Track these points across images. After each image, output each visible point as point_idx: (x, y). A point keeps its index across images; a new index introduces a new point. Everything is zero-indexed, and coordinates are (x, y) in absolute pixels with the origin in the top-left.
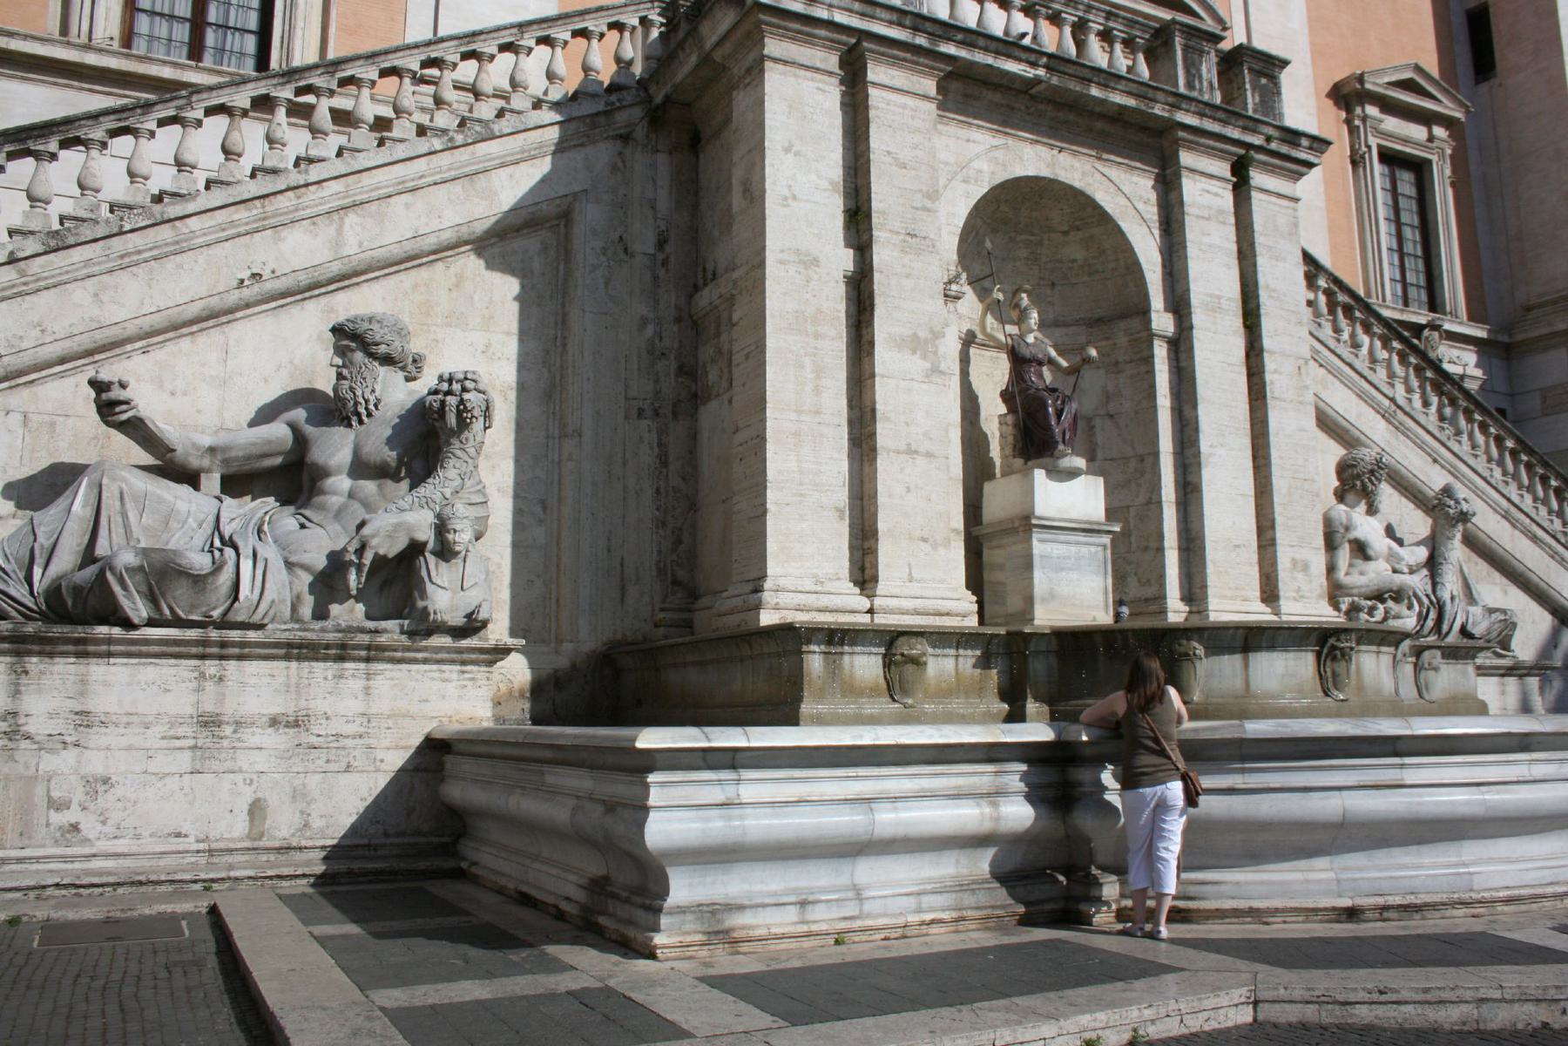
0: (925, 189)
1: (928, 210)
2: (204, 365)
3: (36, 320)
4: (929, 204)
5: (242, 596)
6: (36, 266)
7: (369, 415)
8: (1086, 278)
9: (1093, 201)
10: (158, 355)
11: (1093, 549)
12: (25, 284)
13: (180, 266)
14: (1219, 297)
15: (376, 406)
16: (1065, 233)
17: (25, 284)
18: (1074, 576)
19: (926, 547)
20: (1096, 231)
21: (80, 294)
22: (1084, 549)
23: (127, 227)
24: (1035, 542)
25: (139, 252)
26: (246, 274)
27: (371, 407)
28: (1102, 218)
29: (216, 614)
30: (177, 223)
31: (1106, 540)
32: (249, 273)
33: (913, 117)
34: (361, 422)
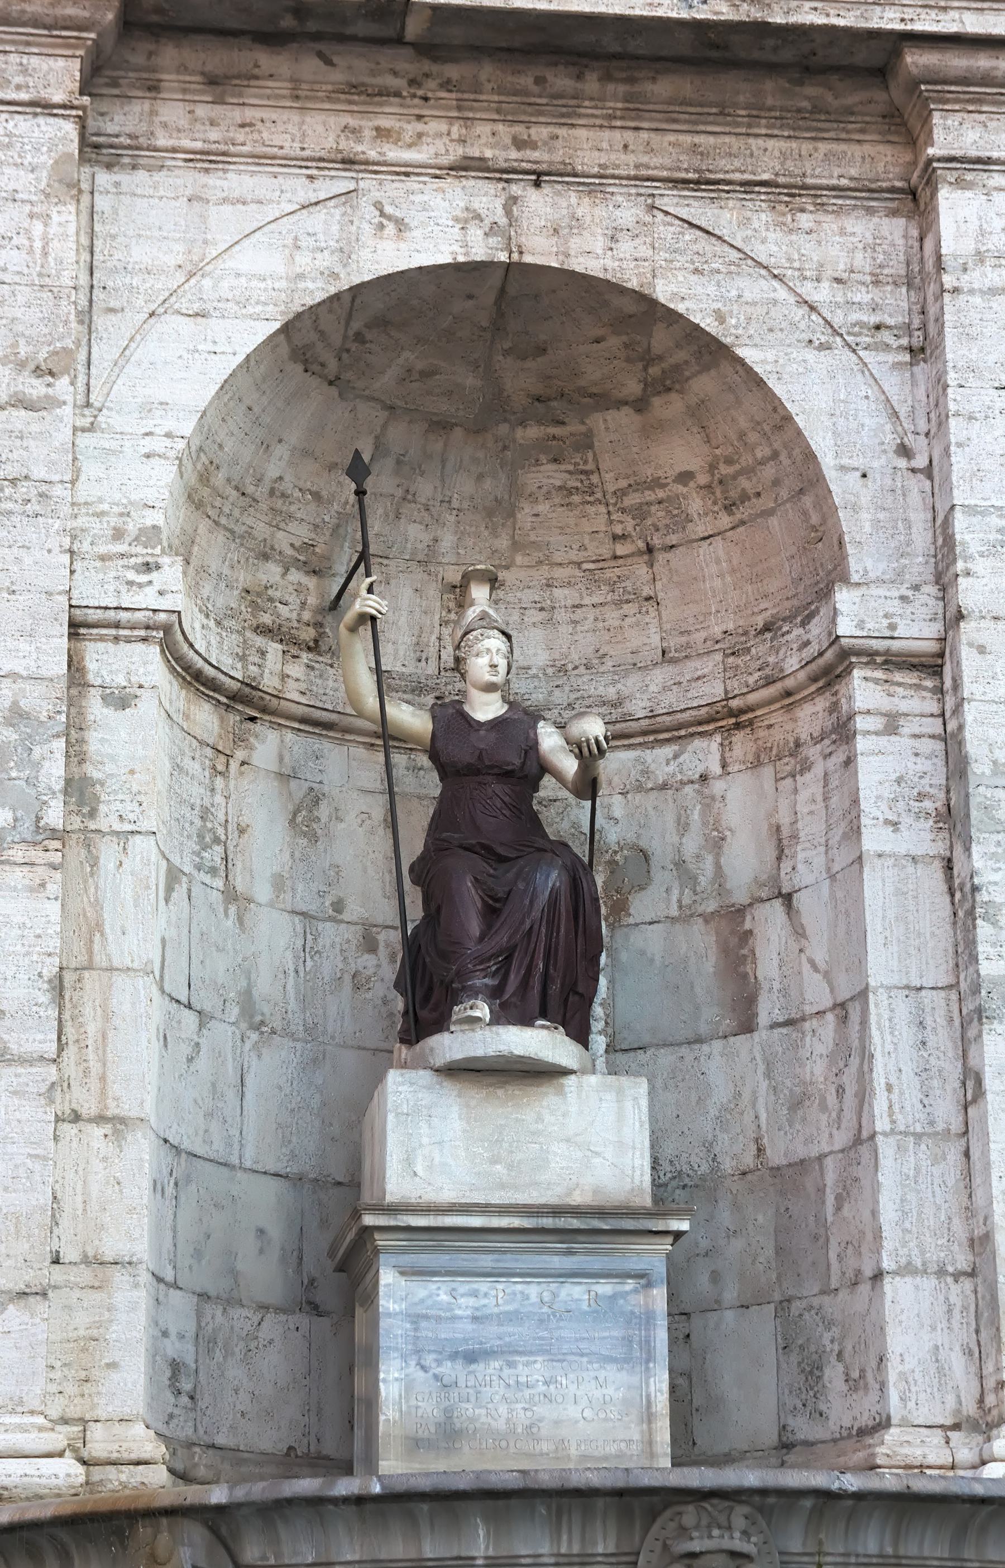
4: (36, 388)
8: (725, 520)
11: (605, 1288)
18: (534, 1371)
22: (575, 1292)
24: (387, 1277)
31: (653, 1256)
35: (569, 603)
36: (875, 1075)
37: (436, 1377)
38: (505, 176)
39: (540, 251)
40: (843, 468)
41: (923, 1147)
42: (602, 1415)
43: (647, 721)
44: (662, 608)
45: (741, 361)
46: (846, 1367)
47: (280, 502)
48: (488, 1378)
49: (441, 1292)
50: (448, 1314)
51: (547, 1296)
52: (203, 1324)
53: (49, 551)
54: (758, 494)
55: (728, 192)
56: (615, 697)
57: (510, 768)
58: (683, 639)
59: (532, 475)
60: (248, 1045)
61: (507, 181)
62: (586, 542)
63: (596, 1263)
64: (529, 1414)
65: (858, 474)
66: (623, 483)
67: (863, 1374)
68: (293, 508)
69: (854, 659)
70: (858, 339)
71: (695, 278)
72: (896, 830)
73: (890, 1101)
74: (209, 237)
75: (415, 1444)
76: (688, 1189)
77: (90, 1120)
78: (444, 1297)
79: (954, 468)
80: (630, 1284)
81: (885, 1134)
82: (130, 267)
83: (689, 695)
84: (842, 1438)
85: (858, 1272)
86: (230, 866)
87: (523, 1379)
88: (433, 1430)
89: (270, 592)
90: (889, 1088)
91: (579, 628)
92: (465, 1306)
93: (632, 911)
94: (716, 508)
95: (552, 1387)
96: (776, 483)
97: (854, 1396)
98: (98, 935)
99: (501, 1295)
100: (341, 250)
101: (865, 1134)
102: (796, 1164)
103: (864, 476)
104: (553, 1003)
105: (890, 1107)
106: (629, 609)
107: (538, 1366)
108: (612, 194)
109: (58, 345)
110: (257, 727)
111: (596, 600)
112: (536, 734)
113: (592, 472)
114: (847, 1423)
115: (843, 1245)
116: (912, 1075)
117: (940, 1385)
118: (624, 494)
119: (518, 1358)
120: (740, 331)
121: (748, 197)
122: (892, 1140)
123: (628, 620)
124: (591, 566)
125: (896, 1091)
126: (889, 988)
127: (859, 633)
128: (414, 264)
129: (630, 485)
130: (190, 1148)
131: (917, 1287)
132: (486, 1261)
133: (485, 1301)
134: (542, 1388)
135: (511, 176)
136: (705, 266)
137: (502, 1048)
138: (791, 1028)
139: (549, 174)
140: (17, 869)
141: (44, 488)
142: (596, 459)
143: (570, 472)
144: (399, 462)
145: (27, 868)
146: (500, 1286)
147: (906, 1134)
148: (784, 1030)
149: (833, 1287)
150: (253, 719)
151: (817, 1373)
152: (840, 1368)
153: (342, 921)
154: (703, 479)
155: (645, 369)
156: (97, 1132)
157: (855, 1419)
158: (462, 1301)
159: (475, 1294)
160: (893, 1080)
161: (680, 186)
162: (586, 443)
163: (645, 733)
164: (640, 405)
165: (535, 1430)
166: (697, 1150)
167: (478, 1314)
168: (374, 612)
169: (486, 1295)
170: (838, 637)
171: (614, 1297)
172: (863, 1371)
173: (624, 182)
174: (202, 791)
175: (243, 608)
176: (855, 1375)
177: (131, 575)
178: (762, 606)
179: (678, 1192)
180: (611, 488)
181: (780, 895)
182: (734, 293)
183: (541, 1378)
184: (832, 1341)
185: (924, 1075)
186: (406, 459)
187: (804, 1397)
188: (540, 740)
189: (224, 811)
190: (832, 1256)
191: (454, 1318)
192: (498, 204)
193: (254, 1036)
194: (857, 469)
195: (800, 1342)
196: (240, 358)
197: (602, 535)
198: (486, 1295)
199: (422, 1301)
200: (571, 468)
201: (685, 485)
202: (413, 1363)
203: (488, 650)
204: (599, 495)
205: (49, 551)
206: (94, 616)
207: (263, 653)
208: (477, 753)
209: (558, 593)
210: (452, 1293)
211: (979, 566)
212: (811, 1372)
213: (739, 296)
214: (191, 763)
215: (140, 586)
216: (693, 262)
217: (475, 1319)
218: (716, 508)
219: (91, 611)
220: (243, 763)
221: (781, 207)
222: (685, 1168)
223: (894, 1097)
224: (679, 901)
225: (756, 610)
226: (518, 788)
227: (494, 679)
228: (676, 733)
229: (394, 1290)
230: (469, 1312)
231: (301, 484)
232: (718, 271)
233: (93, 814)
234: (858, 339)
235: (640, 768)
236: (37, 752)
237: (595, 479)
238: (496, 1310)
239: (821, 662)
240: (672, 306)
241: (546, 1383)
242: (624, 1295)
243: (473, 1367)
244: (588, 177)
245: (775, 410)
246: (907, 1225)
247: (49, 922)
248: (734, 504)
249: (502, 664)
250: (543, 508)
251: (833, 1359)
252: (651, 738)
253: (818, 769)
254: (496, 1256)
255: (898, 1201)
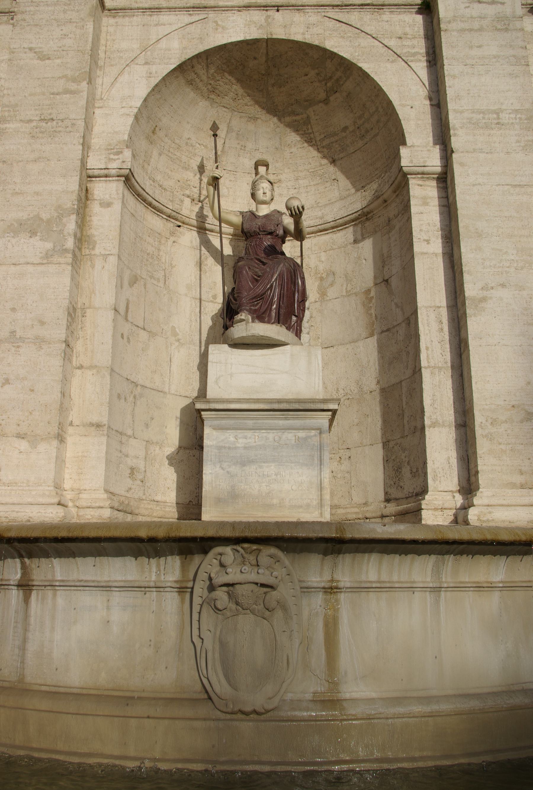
0: (69, 73)
1: (72, 92)
4: (73, 86)
8: (360, 143)
9: (325, 50)
11: (302, 434)
14: (497, 113)
16: (326, 101)
18: (271, 469)
19: (24, 445)
20: (349, 85)
22: (289, 436)
24: (207, 431)
28: (347, 67)
33: (65, 12)
35: (305, 185)
36: (421, 343)
37: (228, 472)
38: (265, 8)
39: (279, 34)
40: (404, 106)
41: (442, 373)
42: (300, 488)
43: (333, 223)
44: (339, 182)
45: (360, 69)
46: (411, 467)
47: (191, 148)
48: (250, 473)
49: (231, 437)
50: (234, 446)
51: (277, 438)
52: (149, 453)
53: (74, 145)
54: (372, 129)
55: (354, 9)
56: (321, 215)
57: (270, 231)
58: (347, 193)
59: (288, 137)
60: (173, 347)
61: (267, 10)
62: (310, 161)
63: (297, 423)
64: (268, 488)
65: (409, 107)
66: (323, 136)
67: (417, 471)
68: (197, 151)
69: (409, 176)
70: (408, 58)
71: (341, 40)
72: (428, 243)
73: (427, 354)
74: (150, 37)
75: (218, 501)
76: (350, 400)
77: (87, 368)
78: (232, 439)
79: (448, 96)
80: (313, 433)
81: (425, 368)
82: (119, 50)
83: (349, 210)
84: (409, 497)
85: (415, 427)
86: (167, 279)
87: (266, 473)
88: (226, 495)
89: (188, 182)
90: (427, 349)
91: (309, 194)
92: (241, 442)
93: (328, 295)
94: (357, 139)
95: (279, 476)
96: (378, 121)
97: (414, 479)
98: (93, 295)
99: (257, 438)
100: (201, 38)
101: (417, 369)
102: (391, 386)
103: (412, 107)
104: (281, 318)
105: (428, 356)
106: (328, 184)
107: (272, 467)
108: (308, 12)
109: (83, 70)
110: (181, 229)
111: (315, 183)
112: (281, 219)
113: (311, 133)
114: (411, 491)
115: (410, 417)
116: (437, 343)
117: (451, 473)
118: (324, 140)
119: (264, 464)
120: (359, 58)
121: (362, 10)
122: (428, 370)
123: (327, 189)
124: (313, 170)
125: (430, 349)
126: (427, 307)
127: (410, 165)
128: (230, 41)
129: (325, 136)
130: (143, 384)
131: (440, 432)
132: (250, 423)
133: (249, 440)
134: (274, 477)
135: (268, 8)
136: (345, 35)
137: (254, 332)
138: (388, 332)
139: (281, 6)
140: (53, 266)
141: (74, 122)
142: (312, 128)
143: (303, 134)
144: (237, 134)
145: (57, 265)
146: (256, 434)
147: (434, 367)
148: (386, 333)
149: (406, 435)
150: (179, 226)
151: (400, 470)
152: (409, 468)
153: (216, 303)
154: (351, 129)
155: (326, 84)
156: (89, 373)
157: (414, 489)
158: (240, 441)
159: (246, 438)
160: (429, 345)
161: (335, 8)
162: (307, 121)
163: (333, 228)
164: (326, 101)
165: (271, 495)
166: (353, 384)
167: (247, 446)
168: (217, 176)
169: (250, 438)
170: (402, 167)
171: (306, 439)
172: (417, 469)
173: (313, 8)
174: (153, 249)
175: (177, 187)
176: (414, 470)
177: (112, 156)
178: (376, 173)
179: (346, 401)
180: (318, 139)
181: (384, 280)
182: (357, 44)
183: (274, 473)
184: (405, 457)
185: (442, 343)
186: (240, 133)
187: (394, 480)
188: (283, 220)
189: (164, 258)
190: (405, 422)
191: (236, 448)
192: (263, 18)
193: (177, 344)
194: (408, 105)
195: (393, 458)
196: (160, 78)
197: (316, 158)
198: (250, 438)
199: (223, 440)
200: (303, 132)
201: (345, 132)
202: (218, 466)
203: (263, 188)
204: (314, 142)
205: (74, 145)
206: (96, 172)
207: (182, 201)
208: (257, 226)
209: (301, 182)
210: (236, 437)
211: (460, 132)
212: (397, 470)
213: (359, 45)
214: (148, 238)
215: (115, 160)
216: (340, 34)
217: (245, 448)
218: (357, 139)
219: (95, 170)
220: (174, 242)
221: (376, 14)
222: (349, 391)
223: (429, 352)
224: (346, 289)
225: (373, 175)
226: (274, 240)
227: (265, 199)
228: (345, 226)
229: (211, 437)
230: (243, 445)
231: (199, 142)
232: (350, 37)
233: (93, 249)
234: (408, 58)
235: (331, 241)
236: (65, 220)
237: (312, 136)
238: (254, 444)
239: (396, 182)
240: (332, 50)
241: (276, 475)
242: (310, 437)
243: (244, 468)
244: (298, 6)
245: (375, 87)
246: (435, 406)
247: (65, 286)
248: (363, 136)
249: (269, 194)
250: (294, 150)
251: (406, 464)
252: (335, 230)
253: (397, 228)
254: (254, 421)
255: (432, 396)
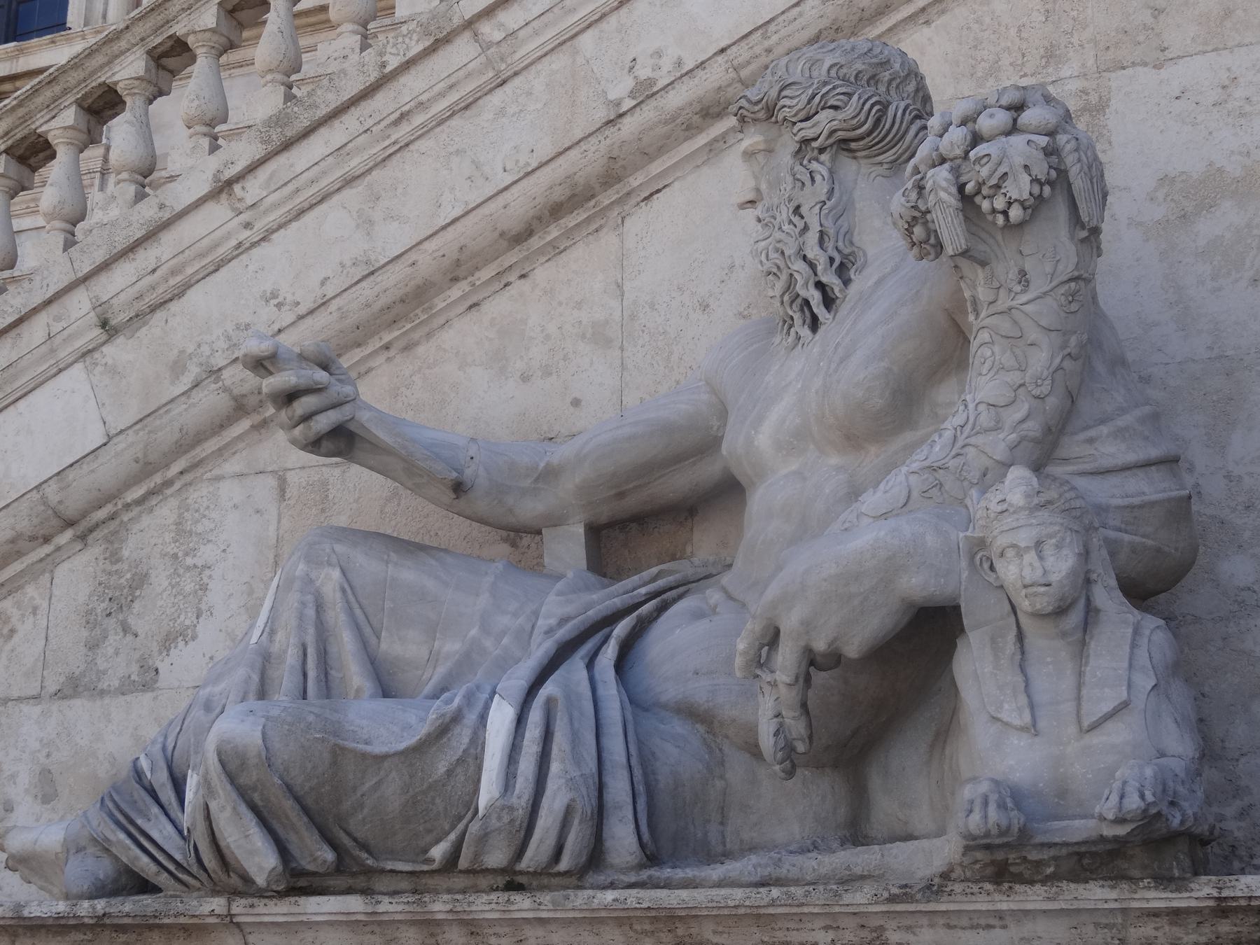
2: (579, 305)
3: (268, 288)
5: (484, 800)
6: (252, 190)
7: (829, 302)
10: (499, 306)
12: (248, 225)
13: (501, 112)
15: (842, 270)
17: (248, 225)
21: (334, 219)
23: (393, 63)
25: (421, 106)
26: (620, 89)
27: (830, 278)
29: (438, 852)
30: (486, 28)
32: (629, 83)
34: (815, 324)
